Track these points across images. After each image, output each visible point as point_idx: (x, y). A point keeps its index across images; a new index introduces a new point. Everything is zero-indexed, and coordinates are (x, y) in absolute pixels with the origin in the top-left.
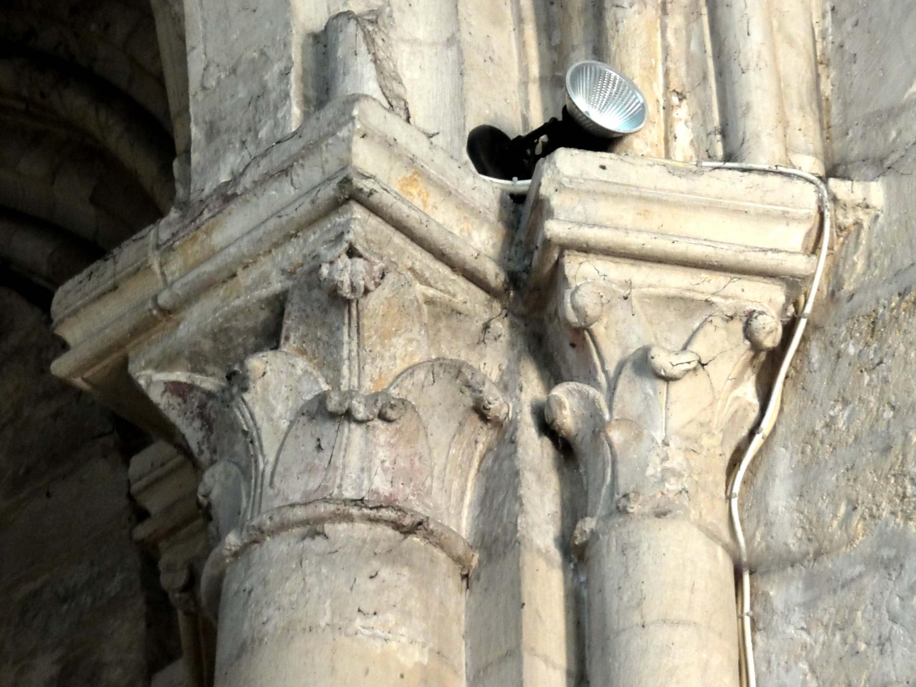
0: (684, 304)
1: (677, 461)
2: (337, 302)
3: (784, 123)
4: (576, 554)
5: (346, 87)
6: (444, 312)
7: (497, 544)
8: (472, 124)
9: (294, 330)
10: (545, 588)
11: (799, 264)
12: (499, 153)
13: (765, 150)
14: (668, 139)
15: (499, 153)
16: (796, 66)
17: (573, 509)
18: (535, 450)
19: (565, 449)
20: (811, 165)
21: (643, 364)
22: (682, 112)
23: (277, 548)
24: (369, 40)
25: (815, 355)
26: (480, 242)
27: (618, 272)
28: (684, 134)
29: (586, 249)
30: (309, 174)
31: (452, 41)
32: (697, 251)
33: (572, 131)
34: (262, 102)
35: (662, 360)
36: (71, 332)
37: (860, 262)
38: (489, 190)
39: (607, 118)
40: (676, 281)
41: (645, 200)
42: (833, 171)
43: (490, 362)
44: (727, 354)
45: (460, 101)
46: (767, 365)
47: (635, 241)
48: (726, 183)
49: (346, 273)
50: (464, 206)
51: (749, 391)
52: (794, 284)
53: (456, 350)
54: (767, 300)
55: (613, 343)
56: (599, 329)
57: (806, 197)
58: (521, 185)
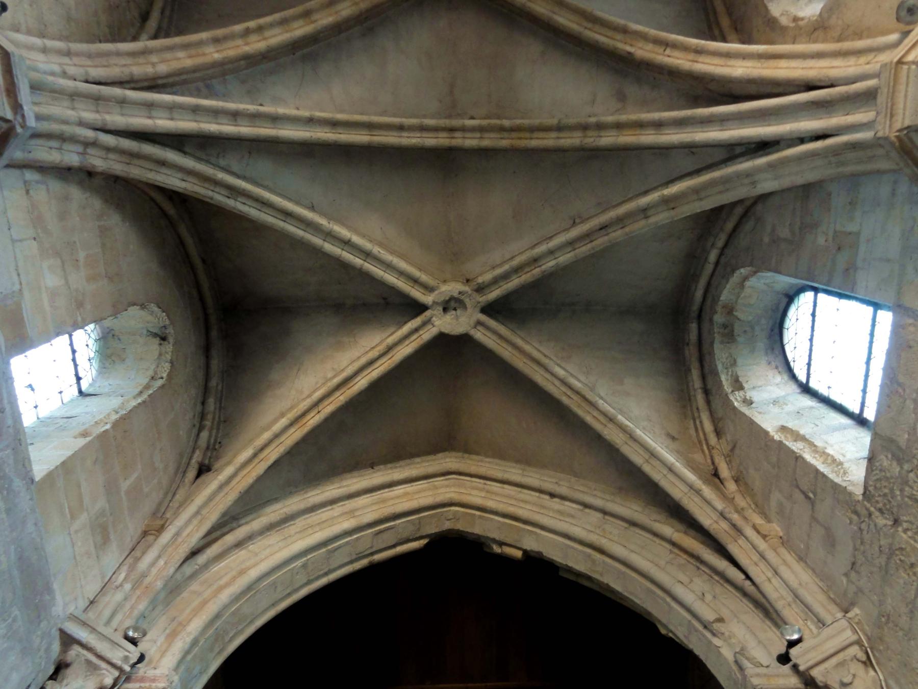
0: (841, 664)
3: (828, 611)
5: (744, 667)
8: (775, 657)
11: (855, 638)
12: (784, 659)
13: (828, 619)
14: (811, 630)
15: (784, 659)
16: (821, 597)
20: (839, 615)
22: (809, 623)
24: (743, 655)
25: (877, 655)
27: (821, 668)
28: (813, 627)
29: (812, 667)
31: (760, 642)
32: (832, 651)
33: (792, 644)
35: (847, 680)
37: (867, 628)
38: (786, 668)
39: (795, 637)
40: (834, 661)
41: (814, 648)
44: (858, 669)
46: (868, 663)
47: (820, 657)
48: (827, 632)
50: (784, 676)
51: (872, 673)
52: (859, 642)
56: (829, 683)
57: (844, 622)
58: (791, 664)
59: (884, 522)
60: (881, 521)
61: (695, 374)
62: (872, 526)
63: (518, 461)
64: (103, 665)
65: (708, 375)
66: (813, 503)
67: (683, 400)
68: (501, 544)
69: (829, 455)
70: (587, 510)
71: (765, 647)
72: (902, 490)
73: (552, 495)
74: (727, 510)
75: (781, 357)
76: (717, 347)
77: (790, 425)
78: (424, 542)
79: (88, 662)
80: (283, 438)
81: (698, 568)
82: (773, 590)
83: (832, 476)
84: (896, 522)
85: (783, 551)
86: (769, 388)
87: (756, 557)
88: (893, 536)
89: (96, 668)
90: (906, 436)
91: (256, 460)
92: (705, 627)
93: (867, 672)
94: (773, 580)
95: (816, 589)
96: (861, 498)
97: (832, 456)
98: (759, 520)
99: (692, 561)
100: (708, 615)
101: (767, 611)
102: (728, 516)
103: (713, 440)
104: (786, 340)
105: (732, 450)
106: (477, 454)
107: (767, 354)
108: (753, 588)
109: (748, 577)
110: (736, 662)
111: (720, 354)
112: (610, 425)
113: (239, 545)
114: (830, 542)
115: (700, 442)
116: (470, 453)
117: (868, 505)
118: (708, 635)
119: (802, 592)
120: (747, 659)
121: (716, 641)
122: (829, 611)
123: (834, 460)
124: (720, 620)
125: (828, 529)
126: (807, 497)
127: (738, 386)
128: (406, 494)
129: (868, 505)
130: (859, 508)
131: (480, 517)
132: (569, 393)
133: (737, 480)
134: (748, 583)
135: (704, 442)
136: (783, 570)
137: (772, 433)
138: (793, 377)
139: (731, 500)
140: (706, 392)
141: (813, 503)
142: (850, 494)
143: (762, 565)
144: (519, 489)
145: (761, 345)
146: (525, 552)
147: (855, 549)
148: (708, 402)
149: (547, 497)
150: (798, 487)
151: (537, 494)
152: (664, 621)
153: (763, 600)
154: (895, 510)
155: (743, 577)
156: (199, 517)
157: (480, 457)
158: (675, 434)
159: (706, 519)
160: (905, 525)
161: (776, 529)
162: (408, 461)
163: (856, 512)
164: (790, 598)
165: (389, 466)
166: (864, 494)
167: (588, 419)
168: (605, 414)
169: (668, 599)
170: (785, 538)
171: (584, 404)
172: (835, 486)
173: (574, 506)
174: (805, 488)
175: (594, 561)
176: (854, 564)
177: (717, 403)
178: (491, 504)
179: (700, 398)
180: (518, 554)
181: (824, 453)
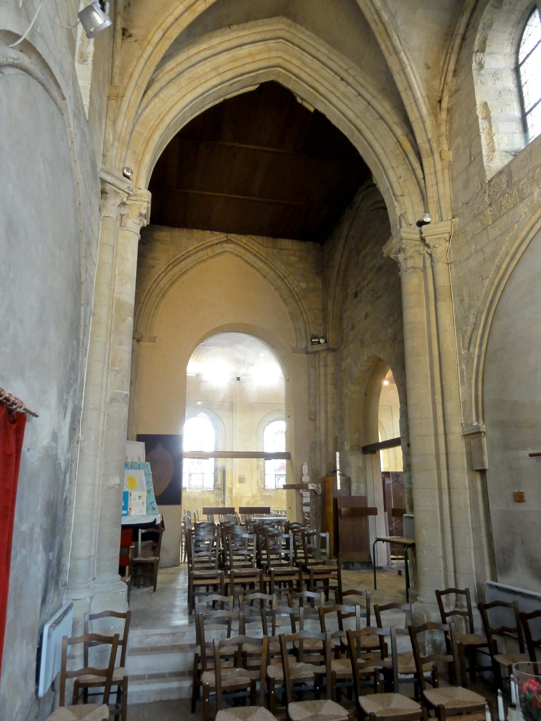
0: (438, 238)
1: (440, 255)
2: (404, 250)
4: (432, 266)
6: (415, 245)
7: (425, 267)
9: (401, 252)
10: (429, 271)
13: (445, 218)
16: (448, 206)
17: (432, 261)
18: (427, 256)
19: (430, 255)
20: (450, 218)
21: (434, 247)
22: (437, 215)
23: (404, 274)
26: (418, 236)
28: (437, 217)
30: (398, 237)
34: (396, 225)
36: (384, 252)
39: (427, 219)
42: (453, 217)
43: (422, 248)
45: (415, 219)
49: (403, 246)
52: (449, 233)
53: (418, 249)
54: (447, 236)
55: (431, 245)
57: (449, 223)
59: (487, 200)
60: (487, 199)
61: (464, 20)
62: (482, 197)
63: (328, 42)
64: (121, 192)
65: (471, 26)
66: (471, 163)
67: (448, 35)
68: (302, 99)
69: (493, 141)
70: (359, 97)
71: (415, 215)
72: (500, 197)
73: (342, 79)
74: (432, 140)
75: (520, 31)
76: (488, 8)
77: (490, 104)
78: (256, 87)
79: (115, 191)
80: (180, 21)
81: (404, 160)
82: (431, 192)
83: (485, 159)
84: (490, 205)
85: (446, 171)
86: (500, 57)
87: (432, 171)
88: (486, 208)
89: (119, 193)
90: (516, 179)
91: (164, 39)
92: (394, 194)
93: (446, 243)
94: (434, 187)
95: (449, 201)
96: (487, 182)
97: (494, 143)
98: (445, 147)
99: (403, 154)
100: (398, 192)
101: (424, 197)
102: (432, 143)
103: (450, 74)
104: (529, 23)
105: (457, 91)
106: (301, 25)
107: (513, 26)
108: (424, 185)
109: (424, 178)
110: (400, 217)
111: (486, 16)
112: (394, 56)
113: (156, 95)
114: (466, 184)
115: (442, 72)
116: (297, 23)
117: (487, 188)
118: (394, 199)
119: (442, 200)
120: (405, 220)
121: (396, 204)
122: (447, 214)
123: (493, 146)
124: (402, 195)
125: (468, 179)
126: (470, 157)
127: (482, 50)
128: (250, 54)
129: (487, 188)
130: (484, 185)
131: (295, 80)
132: (378, 21)
133: (448, 110)
134: (422, 181)
135: (444, 73)
136: (441, 185)
137: (478, 106)
138: (517, 52)
139: (438, 125)
140: (464, 39)
141: (471, 163)
142: (485, 176)
143: (433, 176)
144: (323, 66)
145: (514, 18)
146: (316, 111)
147: (472, 198)
148: (461, 48)
149: (339, 79)
150: (470, 148)
151: (333, 74)
152: (376, 178)
153: (425, 194)
154: (493, 200)
155: (422, 177)
156: (137, 87)
157: (303, 29)
158: (430, 65)
159: (419, 141)
160: (492, 209)
161: (450, 155)
162: (253, 22)
163: (482, 185)
164: (436, 199)
165: (241, 26)
166: (489, 181)
167: (383, 47)
168: (394, 47)
169: (383, 173)
170: (452, 163)
171: (384, 34)
172: (482, 166)
173: (353, 91)
174: (472, 153)
175: (353, 133)
176: (467, 203)
177: (465, 51)
178: (303, 75)
179: (458, 41)
180: (312, 110)
181: (492, 138)
